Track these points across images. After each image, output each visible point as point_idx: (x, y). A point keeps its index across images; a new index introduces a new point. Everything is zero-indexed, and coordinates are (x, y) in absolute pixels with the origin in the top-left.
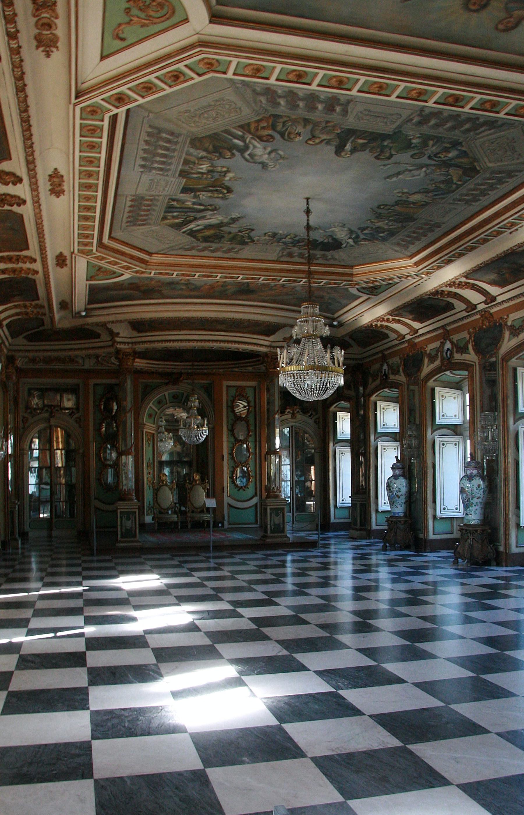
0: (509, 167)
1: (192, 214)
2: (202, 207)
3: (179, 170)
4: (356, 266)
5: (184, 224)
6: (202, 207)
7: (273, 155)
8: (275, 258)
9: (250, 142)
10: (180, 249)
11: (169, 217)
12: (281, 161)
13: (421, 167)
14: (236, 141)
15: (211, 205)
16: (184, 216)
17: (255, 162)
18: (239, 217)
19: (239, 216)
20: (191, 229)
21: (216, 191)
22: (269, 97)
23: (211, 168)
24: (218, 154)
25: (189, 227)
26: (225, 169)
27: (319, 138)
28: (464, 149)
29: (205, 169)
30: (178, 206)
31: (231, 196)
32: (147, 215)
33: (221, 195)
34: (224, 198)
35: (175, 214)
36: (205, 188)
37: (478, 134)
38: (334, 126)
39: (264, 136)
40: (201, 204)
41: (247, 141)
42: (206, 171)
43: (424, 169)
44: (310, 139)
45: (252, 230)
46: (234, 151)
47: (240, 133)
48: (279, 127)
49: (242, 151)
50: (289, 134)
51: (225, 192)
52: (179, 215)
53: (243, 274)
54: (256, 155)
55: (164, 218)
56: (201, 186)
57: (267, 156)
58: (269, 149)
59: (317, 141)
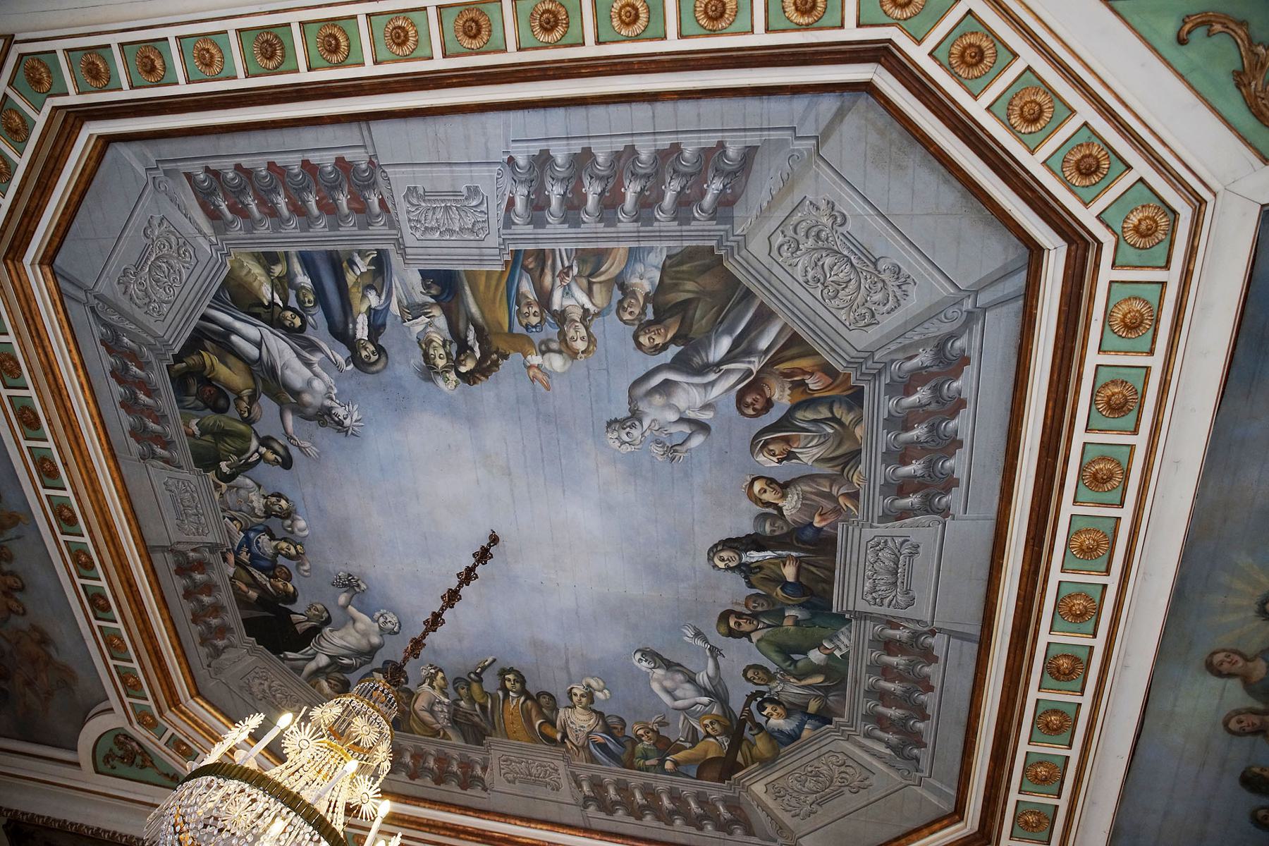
0: (762, 815)
1: (317, 317)
2: (362, 332)
3: (541, 247)
4: (204, 698)
5: (257, 310)
6: (362, 332)
7: (686, 429)
8: (150, 543)
9: (728, 371)
10: (106, 325)
11: (278, 270)
12: (657, 450)
13: (717, 693)
14: (725, 344)
15: (380, 350)
16: (301, 302)
17: (632, 399)
18: (340, 423)
19: (347, 422)
20: (231, 330)
21: (464, 347)
22: (935, 369)
23: (577, 314)
24: (650, 315)
25: (238, 325)
26: (580, 345)
27: (784, 496)
28: (805, 734)
29: (567, 302)
30: (350, 278)
31: (449, 385)
32: (273, 212)
33: (441, 363)
34: (429, 370)
35: (304, 280)
36: (470, 319)
37: (868, 735)
38: (838, 510)
39: (762, 393)
40: (376, 329)
41: (725, 367)
42: (556, 306)
43: (706, 700)
44: (771, 481)
45: (287, 463)
46: (674, 350)
47: (763, 344)
48: (810, 415)
49: (680, 364)
50: (787, 440)
51: (463, 369)
52: (299, 289)
53: (76, 494)
54: (669, 395)
55: (268, 260)
56: (474, 309)
57: (673, 417)
58: (706, 416)
59: (769, 496)
